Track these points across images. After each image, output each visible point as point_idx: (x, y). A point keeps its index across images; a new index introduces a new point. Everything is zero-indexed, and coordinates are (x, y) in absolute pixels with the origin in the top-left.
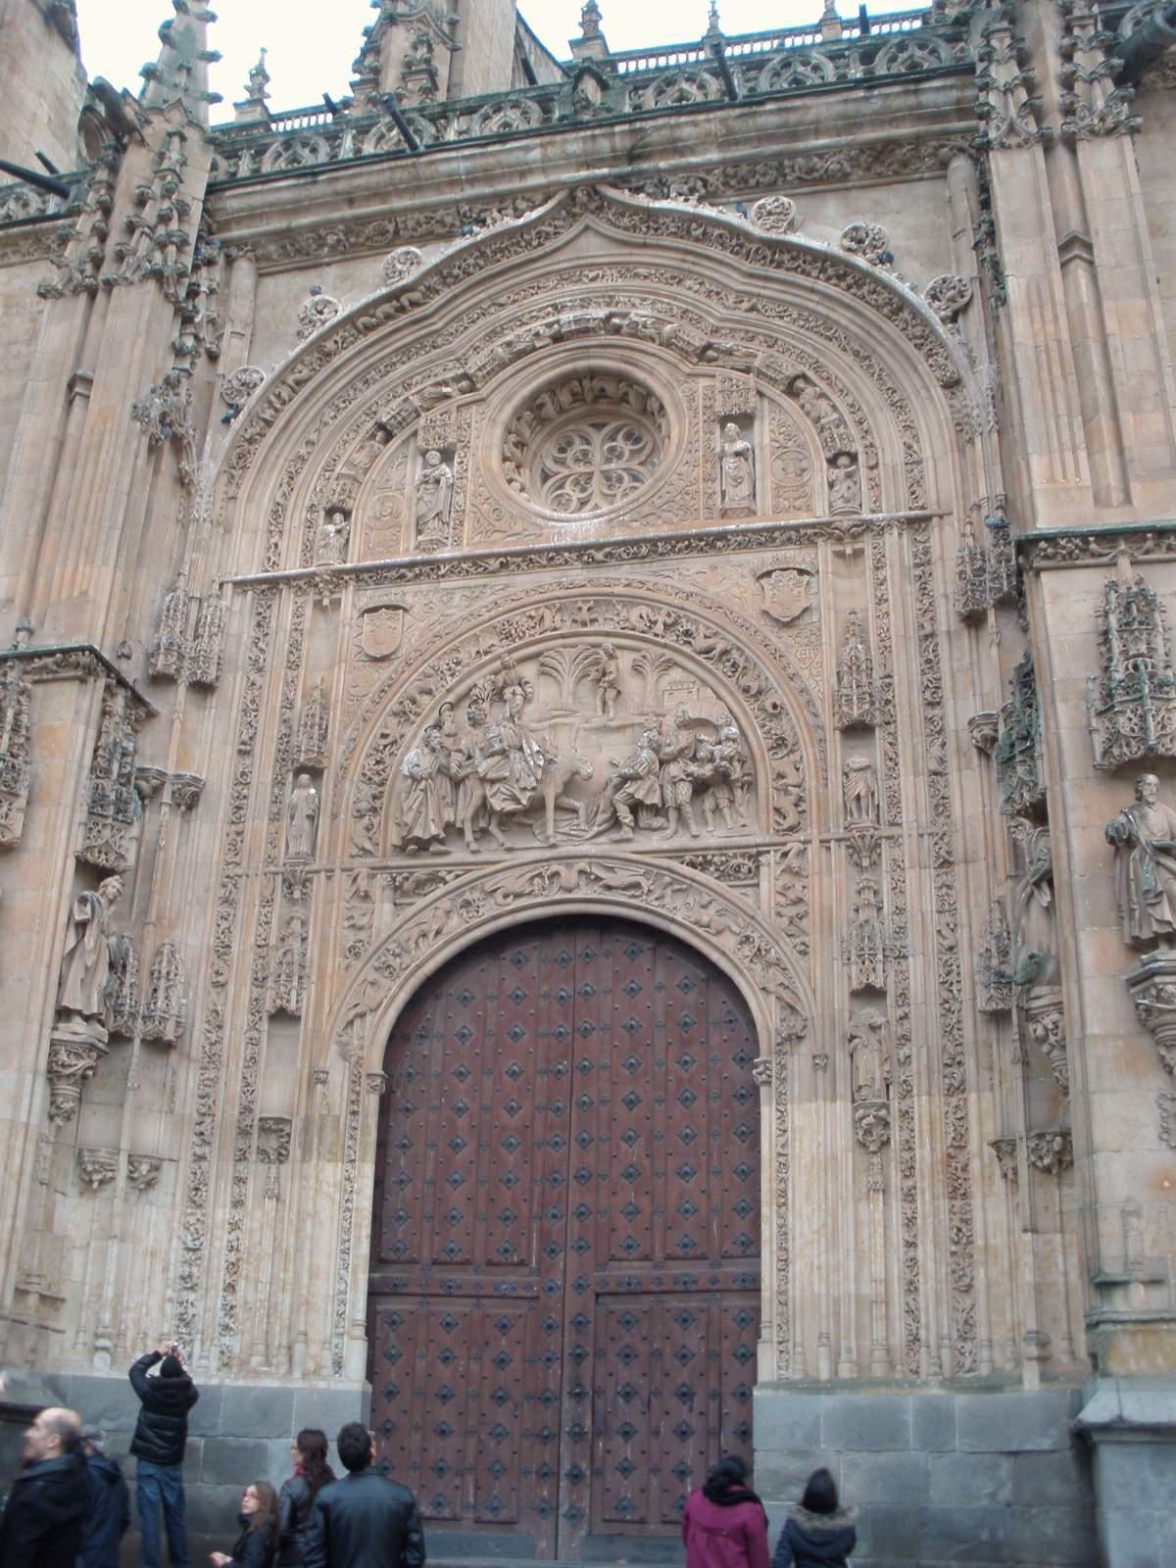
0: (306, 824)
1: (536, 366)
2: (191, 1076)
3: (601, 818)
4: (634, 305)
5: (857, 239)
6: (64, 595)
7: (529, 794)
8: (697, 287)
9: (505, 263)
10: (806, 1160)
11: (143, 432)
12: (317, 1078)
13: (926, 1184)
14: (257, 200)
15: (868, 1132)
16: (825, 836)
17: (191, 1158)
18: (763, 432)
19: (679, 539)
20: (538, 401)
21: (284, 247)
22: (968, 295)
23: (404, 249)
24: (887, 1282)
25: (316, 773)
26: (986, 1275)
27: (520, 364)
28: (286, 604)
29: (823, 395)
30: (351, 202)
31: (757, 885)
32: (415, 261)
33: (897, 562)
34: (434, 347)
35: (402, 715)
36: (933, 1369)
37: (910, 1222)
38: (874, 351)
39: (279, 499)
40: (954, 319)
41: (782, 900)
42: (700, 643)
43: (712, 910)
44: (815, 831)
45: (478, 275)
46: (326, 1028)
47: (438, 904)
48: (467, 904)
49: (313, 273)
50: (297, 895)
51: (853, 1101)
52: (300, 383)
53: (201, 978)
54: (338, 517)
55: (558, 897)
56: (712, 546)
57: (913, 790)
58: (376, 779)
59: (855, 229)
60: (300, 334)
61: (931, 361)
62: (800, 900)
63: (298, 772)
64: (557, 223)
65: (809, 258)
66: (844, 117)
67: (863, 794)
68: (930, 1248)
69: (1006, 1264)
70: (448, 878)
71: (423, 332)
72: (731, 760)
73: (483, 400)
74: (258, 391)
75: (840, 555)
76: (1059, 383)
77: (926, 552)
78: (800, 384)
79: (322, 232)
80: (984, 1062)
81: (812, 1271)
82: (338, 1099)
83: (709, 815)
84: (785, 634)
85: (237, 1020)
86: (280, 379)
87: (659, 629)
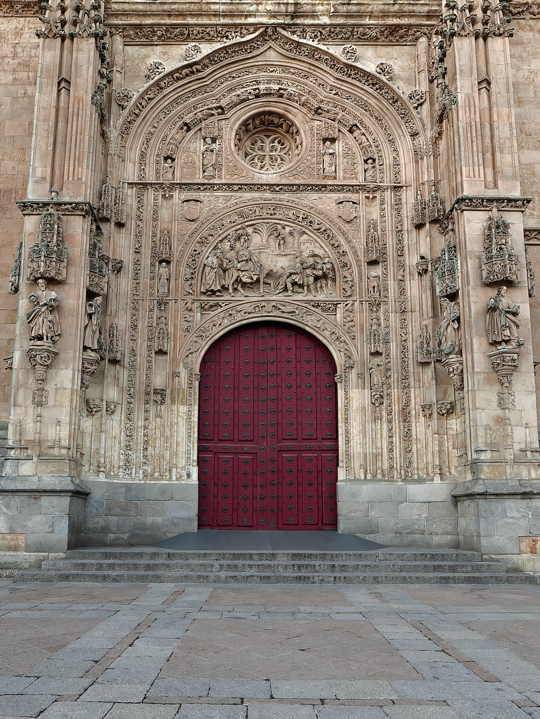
0: (166, 281)
1: (249, 107)
2: (125, 373)
3: (280, 287)
4: (289, 85)
5: (382, 69)
7: (256, 277)
8: (314, 81)
9: (236, 58)
10: (355, 408)
12: (176, 375)
13: (397, 417)
15: (377, 400)
16: (361, 300)
17: (126, 403)
18: (338, 147)
19: (308, 185)
20: (248, 122)
21: (137, 33)
23: (193, 44)
25: (168, 262)
27: (242, 105)
28: (150, 195)
29: (364, 134)
30: (170, 16)
31: (336, 315)
33: (389, 202)
34: (206, 92)
35: (201, 243)
37: (390, 430)
38: (384, 118)
39: (143, 150)
40: (416, 108)
41: (345, 320)
42: (316, 226)
43: (321, 322)
44: (358, 297)
45: (225, 62)
46: (178, 357)
47: (219, 314)
48: (231, 315)
49: (150, 48)
50: (163, 308)
51: (371, 389)
52: (149, 99)
53: (127, 337)
54: (169, 161)
55: (265, 314)
56: (320, 190)
57: (392, 285)
58: (192, 266)
59: (382, 64)
60: (148, 77)
61: (407, 125)
62: (352, 321)
63: (160, 262)
64: (259, 43)
65: (362, 74)
67: (376, 285)
68: (398, 438)
70: (223, 305)
71: (201, 85)
72: (329, 269)
73: (228, 119)
75: (367, 198)
77: (400, 199)
79: (156, 29)
80: (416, 379)
81: (357, 445)
82: (183, 383)
83: (319, 289)
84: (347, 225)
86: (142, 97)
87: (300, 219)
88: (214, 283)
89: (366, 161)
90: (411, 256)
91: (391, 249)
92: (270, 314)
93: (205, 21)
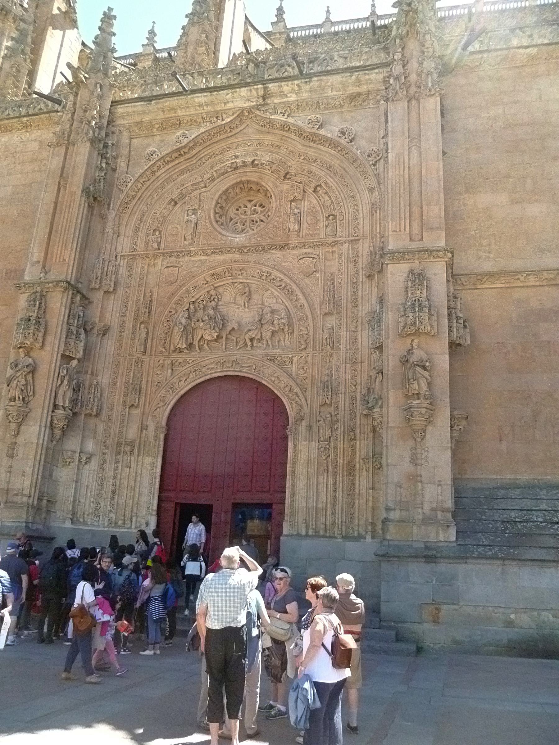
6: (57, 261)
9: (219, 138)
11: (85, 201)
12: (143, 428)
14: (130, 110)
22: (381, 156)
24: (327, 503)
26: (359, 502)
29: (326, 193)
32: (184, 136)
33: (346, 256)
36: (339, 532)
37: (335, 484)
42: (278, 284)
49: (150, 139)
50: (139, 366)
56: (283, 248)
66: (341, 83)
68: (341, 492)
69: (365, 500)
71: (188, 164)
74: (130, 185)
76: (402, 195)
78: (318, 188)
84: (308, 281)
85: (118, 409)
87: (264, 278)
88: (181, 342)
89: (327, 218)
90: (364, 307)
91: (345, 301)
92: (230, 369)
93: (192, 111)
